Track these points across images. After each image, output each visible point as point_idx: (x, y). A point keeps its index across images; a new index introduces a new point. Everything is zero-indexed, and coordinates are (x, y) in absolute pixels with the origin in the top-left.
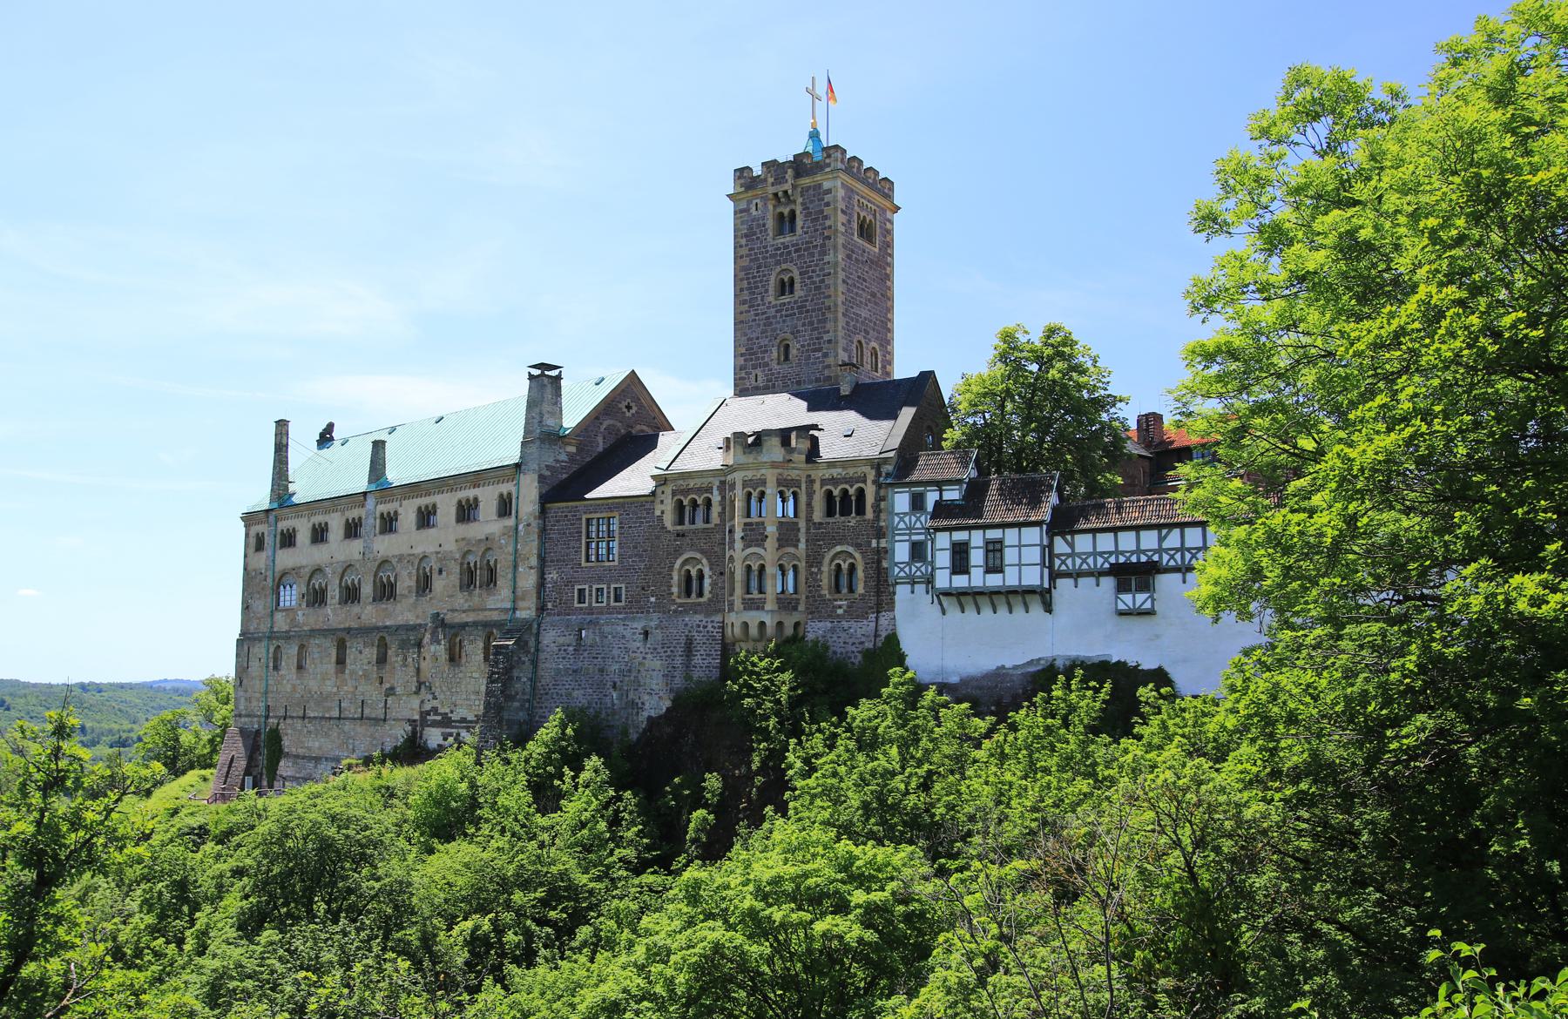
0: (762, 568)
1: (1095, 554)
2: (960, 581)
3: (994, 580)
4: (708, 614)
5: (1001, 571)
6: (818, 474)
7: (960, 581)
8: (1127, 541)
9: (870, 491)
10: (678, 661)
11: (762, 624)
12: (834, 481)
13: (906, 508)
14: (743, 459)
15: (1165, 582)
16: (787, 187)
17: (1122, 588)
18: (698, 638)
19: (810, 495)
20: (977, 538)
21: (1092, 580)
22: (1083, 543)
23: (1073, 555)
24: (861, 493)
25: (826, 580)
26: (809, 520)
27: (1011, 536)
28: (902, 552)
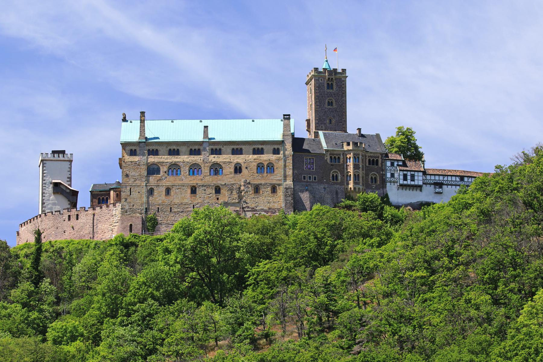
0: (358, 175)
3: (413, 183)
4: (341, 185)
5: (414, 181)
7: (405, 182)
9: (380, 160)
10: (335, 196)
11: (359, 188)
13: (390, 165)
14: (355, 148)
18: (339, 191)
19: (366, 159)
20: (409, 173)
24: (377, 160)
25: (370, 180)
26: (365, 165)
27: (416, 174)
28: (389, 175)
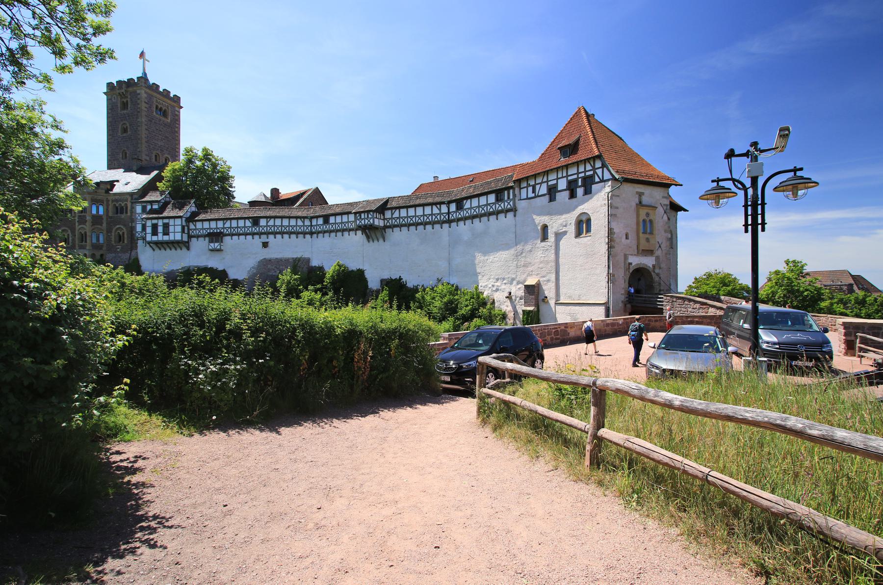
1: (203, 229)
2: (155, 238)
3: (166, 238)
6: (110, 198)
8: (213, 224)
12: (117, 201)
15: (227, 239)
16: (123, 91)
17: (211, 241)
20: (160, 222)
21: (202, 239)
22: (199, 225)
23: (196, 229)
26: (107, 215)
27: (171, 222)
28: (139, 228)
